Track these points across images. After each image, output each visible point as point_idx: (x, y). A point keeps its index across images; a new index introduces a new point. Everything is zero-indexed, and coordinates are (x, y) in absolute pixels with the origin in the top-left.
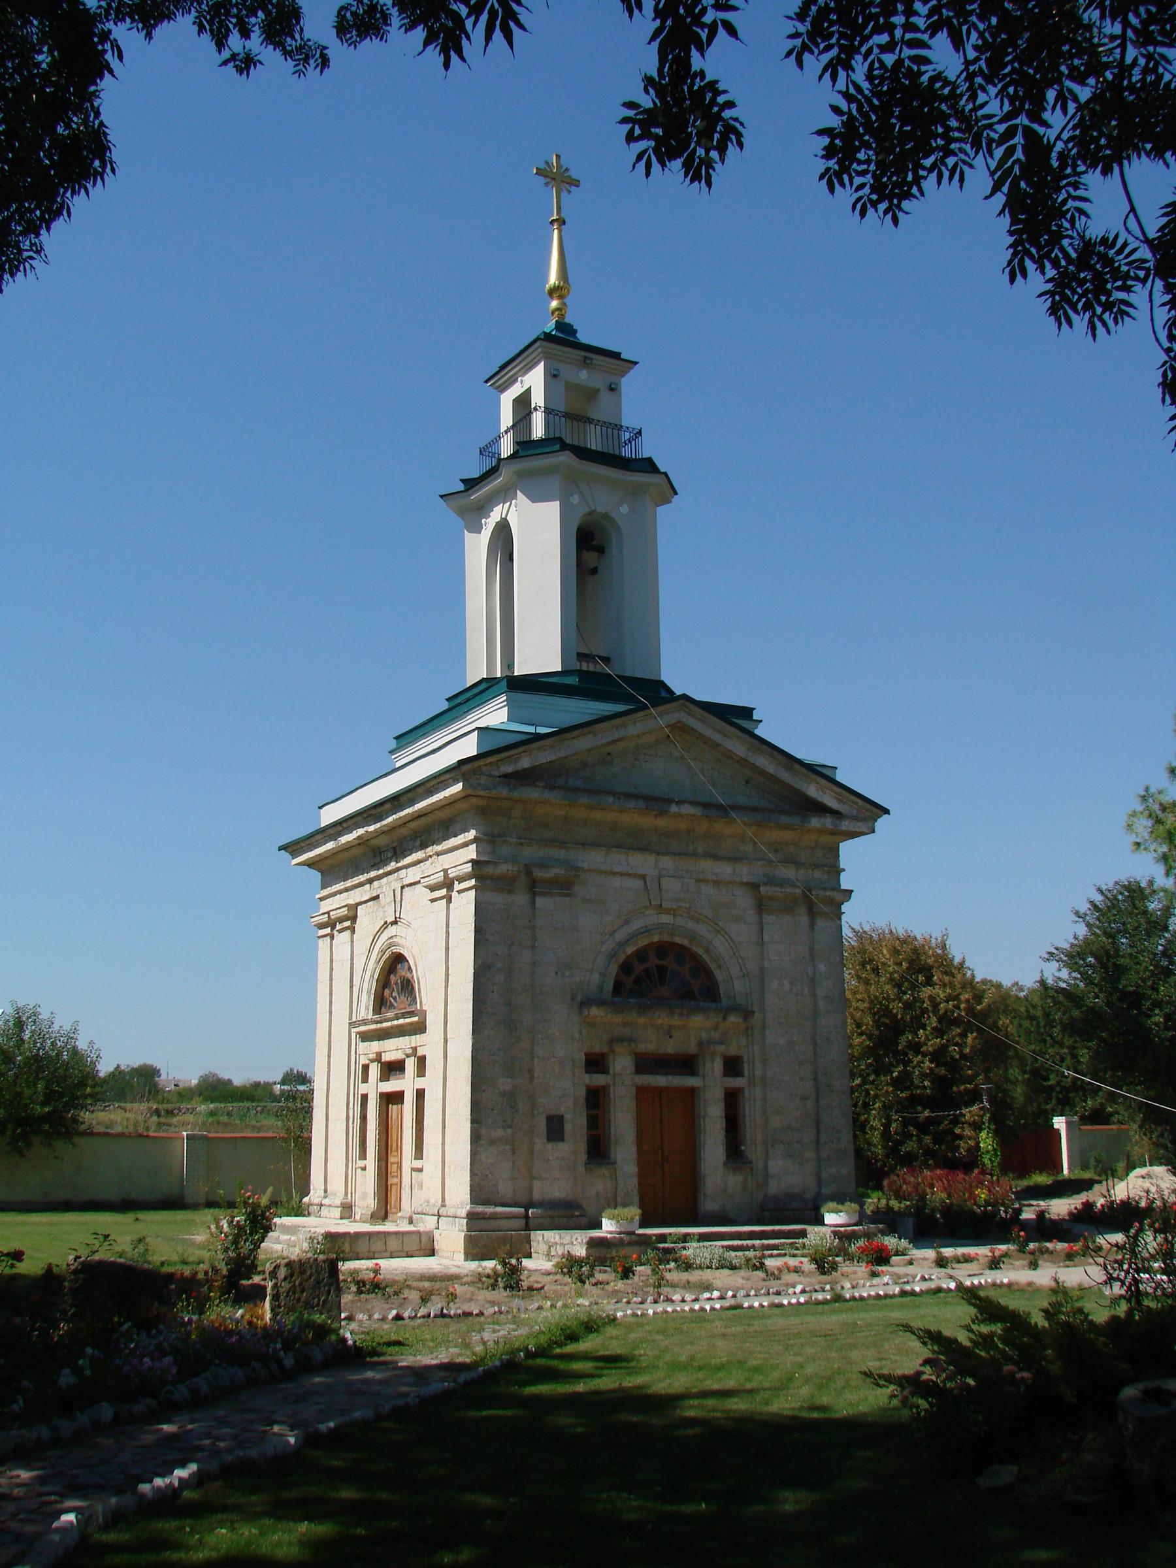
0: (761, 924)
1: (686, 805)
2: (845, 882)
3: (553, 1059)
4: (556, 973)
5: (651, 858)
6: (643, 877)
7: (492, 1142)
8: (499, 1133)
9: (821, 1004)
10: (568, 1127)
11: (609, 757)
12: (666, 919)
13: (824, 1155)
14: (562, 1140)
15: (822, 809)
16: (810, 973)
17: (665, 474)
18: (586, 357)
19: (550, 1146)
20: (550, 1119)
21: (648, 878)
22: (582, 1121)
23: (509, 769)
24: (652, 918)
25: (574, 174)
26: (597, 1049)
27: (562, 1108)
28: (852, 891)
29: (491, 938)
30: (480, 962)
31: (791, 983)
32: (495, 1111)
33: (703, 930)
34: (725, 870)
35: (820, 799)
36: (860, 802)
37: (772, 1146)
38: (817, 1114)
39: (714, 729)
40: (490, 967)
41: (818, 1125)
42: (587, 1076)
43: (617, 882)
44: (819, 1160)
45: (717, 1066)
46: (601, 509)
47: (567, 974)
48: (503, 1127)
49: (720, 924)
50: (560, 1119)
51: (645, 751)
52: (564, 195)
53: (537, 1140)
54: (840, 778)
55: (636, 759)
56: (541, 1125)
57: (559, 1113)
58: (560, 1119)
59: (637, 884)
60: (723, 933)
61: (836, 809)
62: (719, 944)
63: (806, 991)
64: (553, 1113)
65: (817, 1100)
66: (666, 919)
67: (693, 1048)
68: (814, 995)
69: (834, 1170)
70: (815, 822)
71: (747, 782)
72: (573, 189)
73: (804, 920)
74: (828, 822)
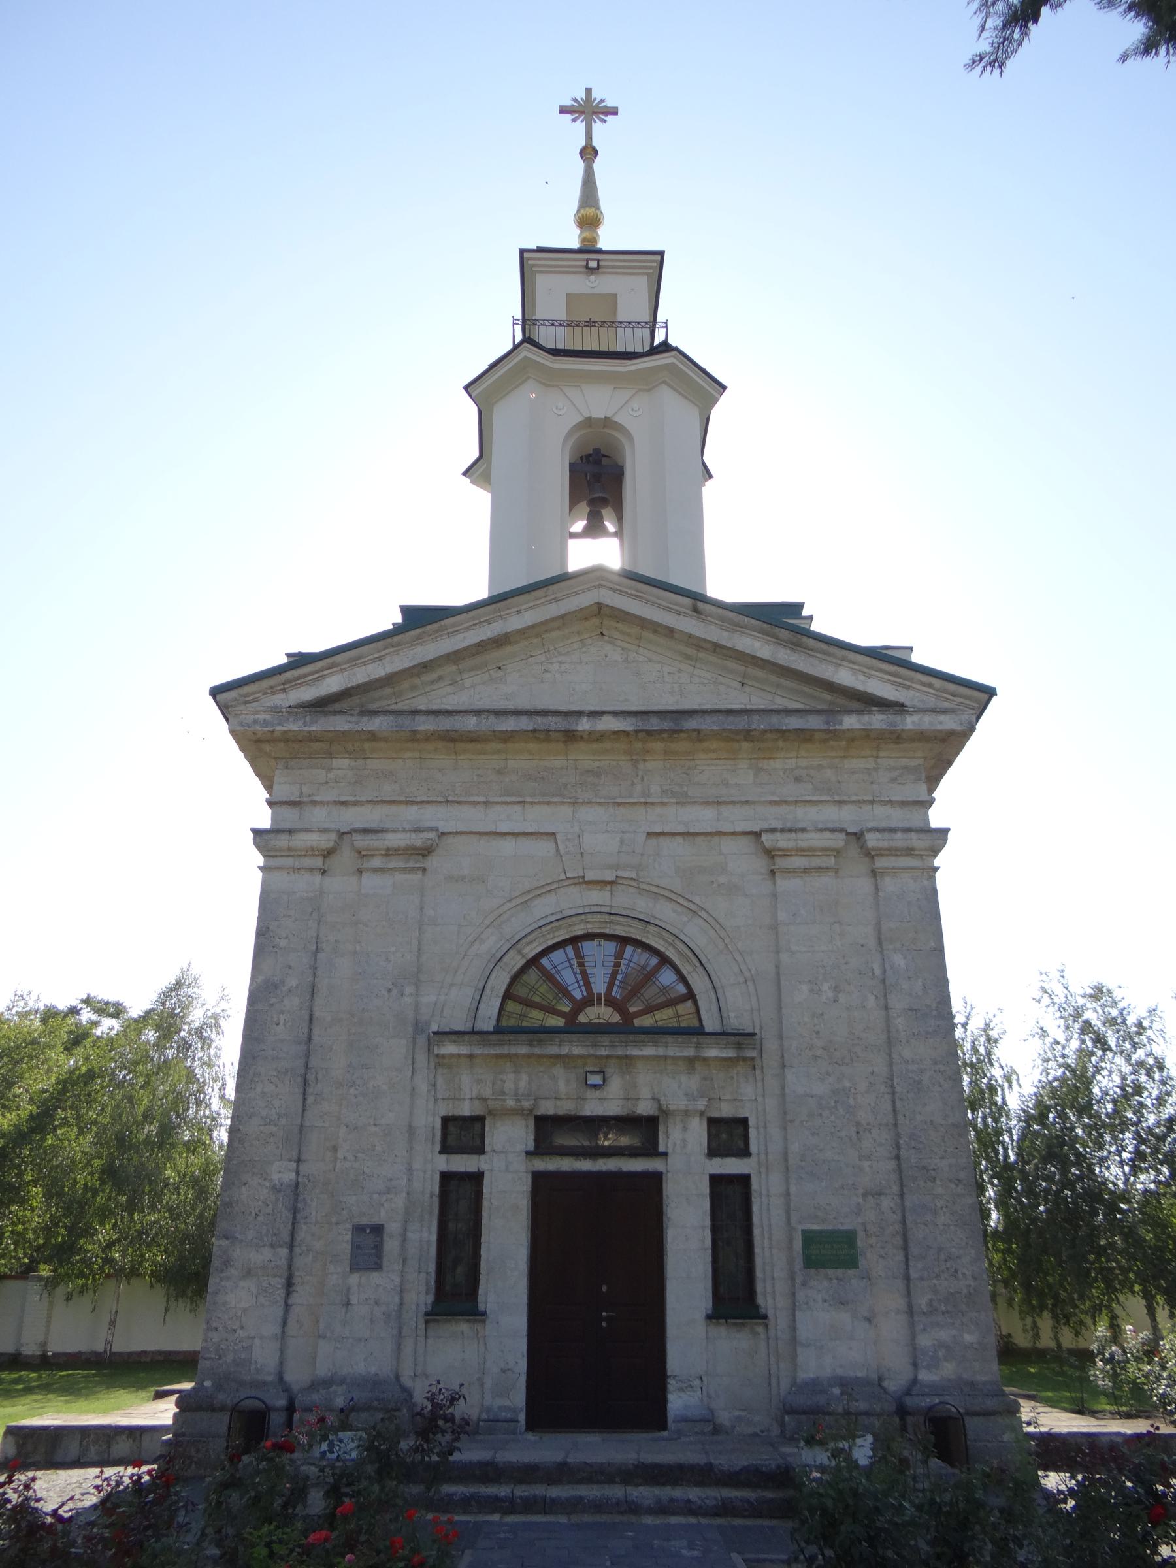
0: (774, 895)
1: (605, 718)
2: (936, 818)
3: (373, 1129)
4: (389, 991)
5: (567, 810)
6: (554, 834)
7: (248, 1273)
8: (260, 1257)
9: (899, 1022)
10: (391, 1246)
11: (501, 673)
12: (597, 897)
13: (922, 1302)
14: (378, 1267)
15: (869, 702)
16: (878, 972)
17: (677, 349)
18: (587, 260)
19: (354, 1279)
20: (359, 1229)
21: (558, 837)
22: (426, 1235)
23: (308, 694)
24: (572, 900)
25: (610, 103)
26: (466, 1110)
27: (383, 1213)
28: (947, 830)
29: (283, 943)
30: (260, 979)
31: (836, 989)
32: (261, 1218)
33: (665, 913)
34: (703, 818)
35: (860, 687)
36: (938, 683)
37: (804, 1284)
38: (903, 1222)
39: (658, 606)
40: (276, 986)
41: (906, 1248)
42: (444, 1157)
43: (508, 846)
44: (910, 1311)
45: (698, 1133)
46: (598, 414)
47: (409, 990)
48: (272, 1246)
49: (697, 900)
50: (378, 1230)
51: (561, 658)
52: (597, 127)
53: (331, 1268)
54: (916, 658)
55: (546, 671)
56: (344, 1238)
57: (376, 1220)
58: (378, 1230)
59: (544, 848)
60: (703, 914)
61: (892, 699)
62: (696, 933)
63: (871, 1002)
64: (364, 1221)
65: (902, 1195)
66: (597, 897)
67: (645, 1108)
68: (886, 1008)
69: (944, 1335)
70: (850, 722)
71: (743, 684)
72: (609, 118)
73: (864, 885)
74: (877, 721)
